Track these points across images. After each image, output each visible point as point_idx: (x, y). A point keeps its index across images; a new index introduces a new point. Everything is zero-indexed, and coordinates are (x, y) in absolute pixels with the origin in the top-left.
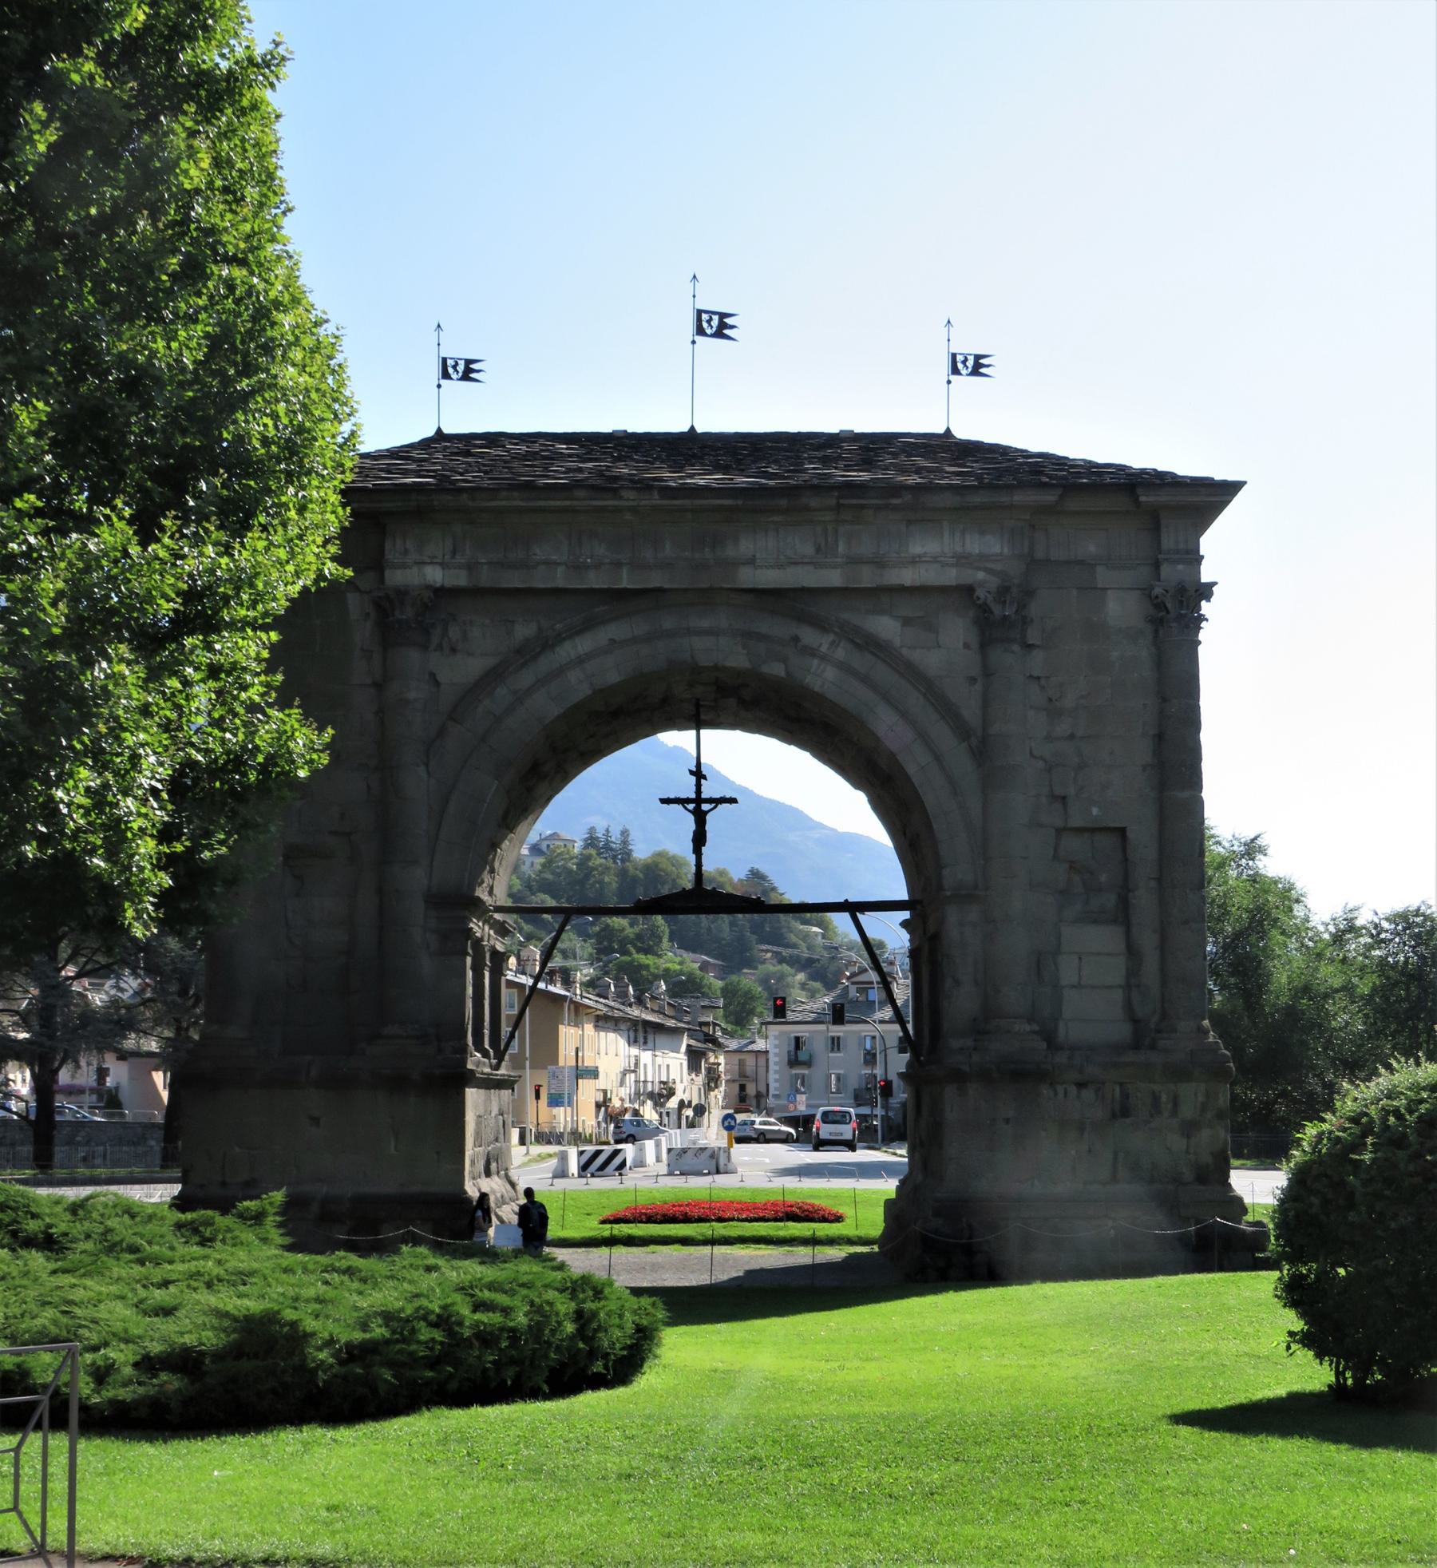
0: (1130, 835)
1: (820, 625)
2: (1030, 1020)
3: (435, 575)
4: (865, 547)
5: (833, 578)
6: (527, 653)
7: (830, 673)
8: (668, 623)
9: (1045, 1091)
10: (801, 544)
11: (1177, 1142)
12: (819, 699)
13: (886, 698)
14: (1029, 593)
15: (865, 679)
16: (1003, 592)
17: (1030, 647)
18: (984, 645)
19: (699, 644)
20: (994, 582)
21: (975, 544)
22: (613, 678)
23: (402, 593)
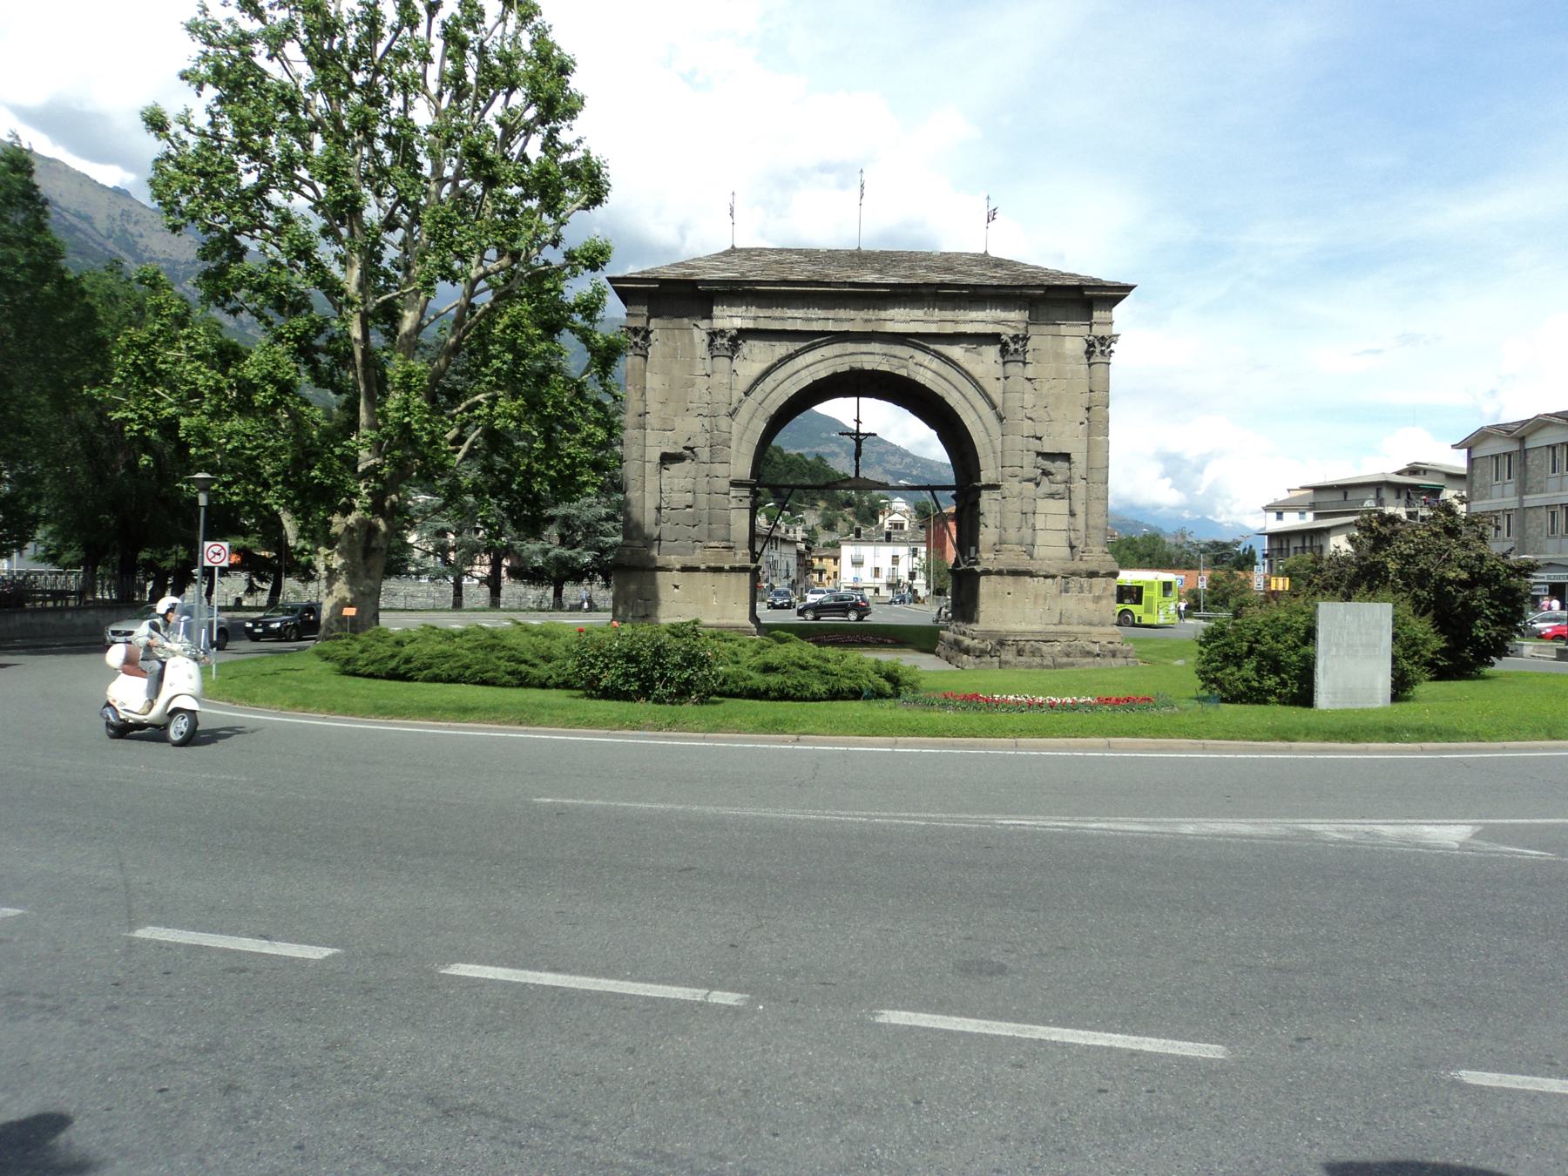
0: (1072, 456)
1: (926, 350)
2: (1020, 544)
3: (738, 323)
4: (948, 315)
5: (933, 329)
6: (784, 361)
7: (929, 374)
8: (850, 347)
9: (1028, 579)
10: (919, 313)
11: (1091, 606)
12: (923, 386)
13: (955, 387)
14: (1026, 338)
15: (945, 379)
16: (1015, 338)
17: (1025, 363)
18: (1004, 363)
19: (865, 358)
20: (1012, 332)
21: (999, 314)
22: (823, 375)
23: (722, 331)
